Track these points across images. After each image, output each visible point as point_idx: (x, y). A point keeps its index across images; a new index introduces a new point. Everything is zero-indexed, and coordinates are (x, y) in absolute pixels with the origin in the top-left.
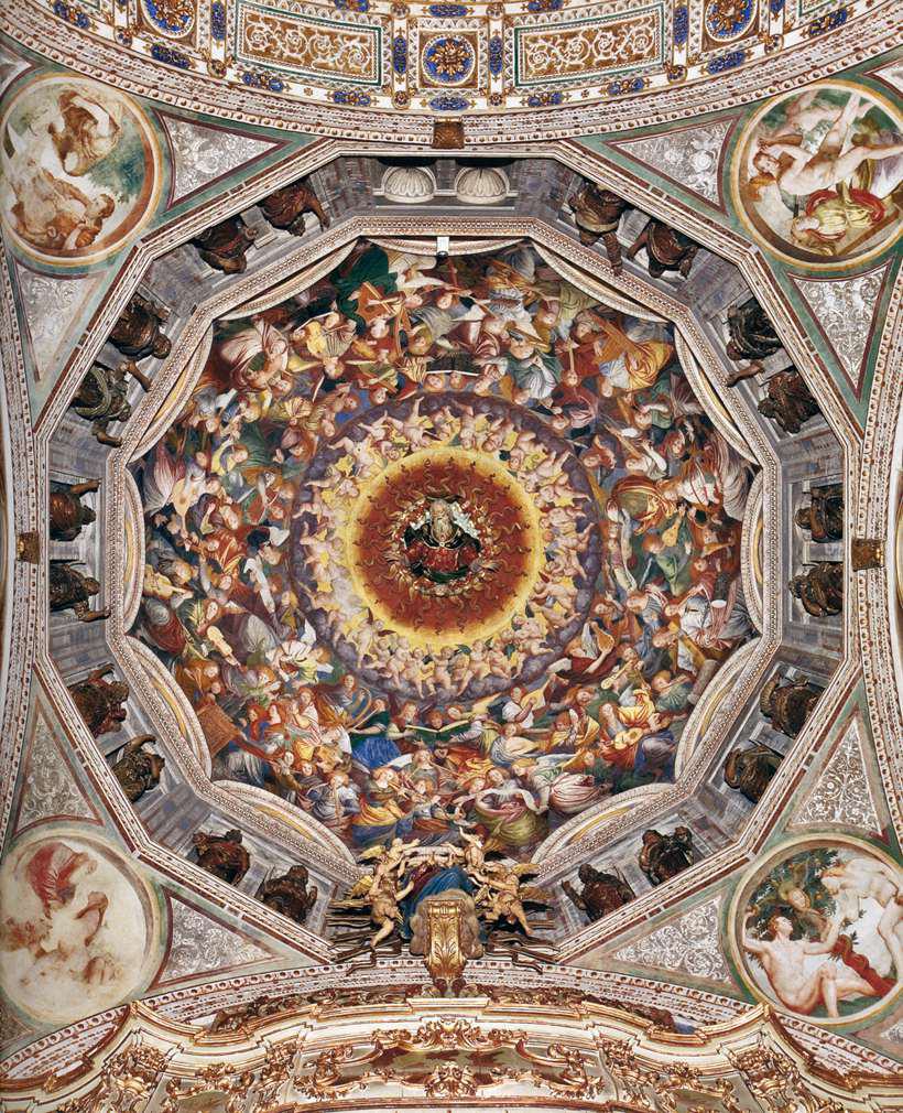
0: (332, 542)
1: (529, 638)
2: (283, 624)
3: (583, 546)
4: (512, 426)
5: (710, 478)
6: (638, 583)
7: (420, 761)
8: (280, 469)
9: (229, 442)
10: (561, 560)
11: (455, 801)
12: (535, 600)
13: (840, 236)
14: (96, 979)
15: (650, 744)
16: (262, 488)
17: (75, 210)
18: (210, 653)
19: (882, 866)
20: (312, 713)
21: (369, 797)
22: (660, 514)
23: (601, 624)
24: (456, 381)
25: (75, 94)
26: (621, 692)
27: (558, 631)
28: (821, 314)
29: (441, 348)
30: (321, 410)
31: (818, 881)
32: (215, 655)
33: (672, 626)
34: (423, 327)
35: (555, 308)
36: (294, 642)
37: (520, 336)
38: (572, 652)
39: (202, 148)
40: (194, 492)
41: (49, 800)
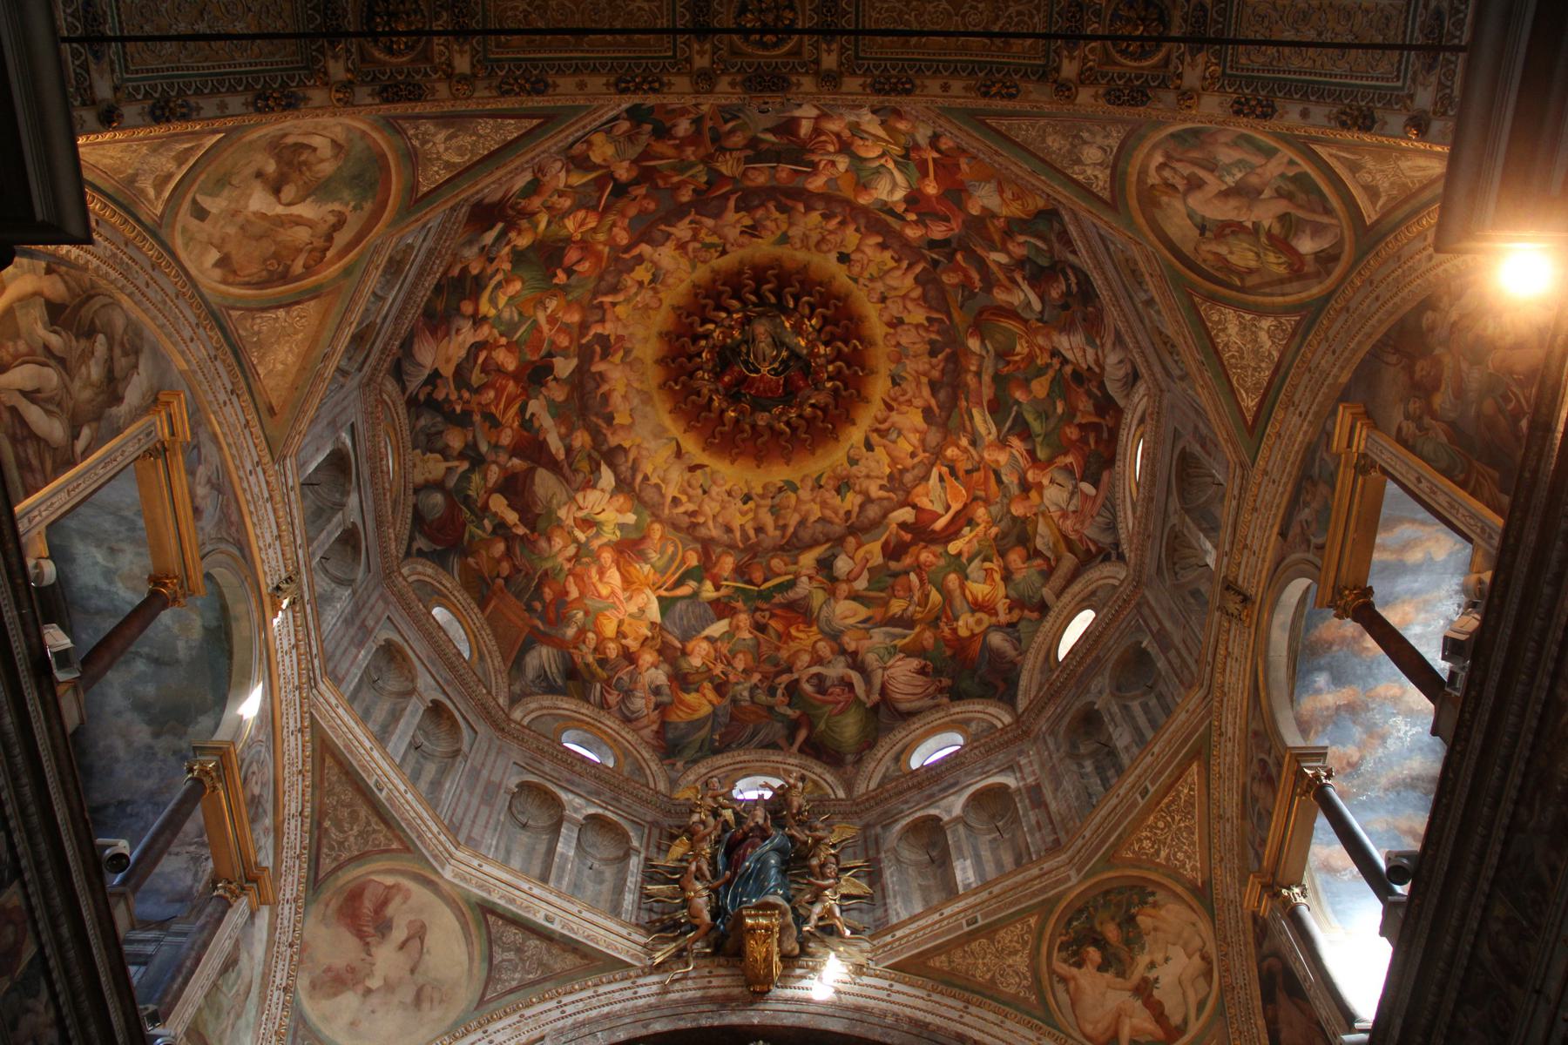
0: (630, 364)
1: (868, 476)
2: (576, 471)
3: (936, 374)
4: (852, 227)
5: (1090, 341)
6: (999, 431)
7: (738, 627)
8: (564, 289)
9: (499, 277)
10: (910, 387)
11: (778, 680)
12: (877, 430)
13: (1251, 271)
14: (426, 1005)
15: (996, 639)
16: (542, 317)
17: (303, 234)
18: (494, 528)
19: (1194, 917)
20: (614, 577)
21: (682, 680)
22: (1031, 358)
23: (953, 472)
24: (784, 175)
25: (285, 135)
26: (970, 560)
27: (902, 472)
28: (1221, 340)
29: (763, 141)
30: (610, 218)
31: (1131, 920)
32: (501, 527)
33: (1033, 494)
36: (589, 491)
38: (917, 500)
39: (449, 138)
40: (460, 346)
41: (352, 839)
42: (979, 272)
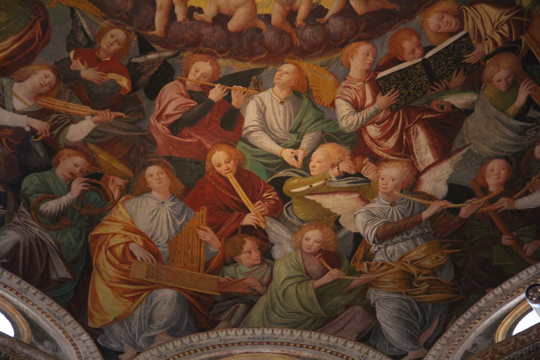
4: (276, 19)
24: (408, 45)
29: (464, 88)
34: (512, 110)
35: (314, 265)
37: (343, 184)
42: (86, 82)
